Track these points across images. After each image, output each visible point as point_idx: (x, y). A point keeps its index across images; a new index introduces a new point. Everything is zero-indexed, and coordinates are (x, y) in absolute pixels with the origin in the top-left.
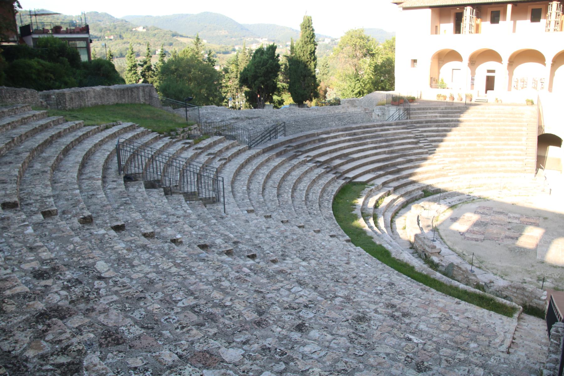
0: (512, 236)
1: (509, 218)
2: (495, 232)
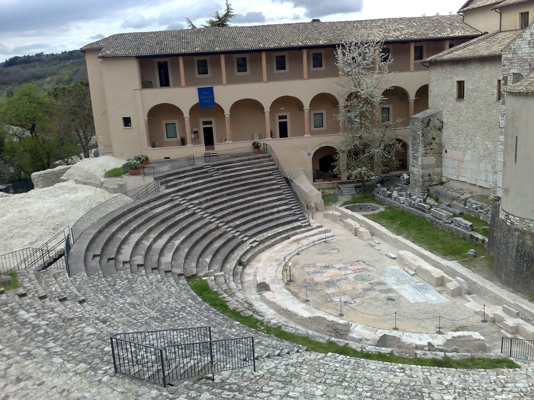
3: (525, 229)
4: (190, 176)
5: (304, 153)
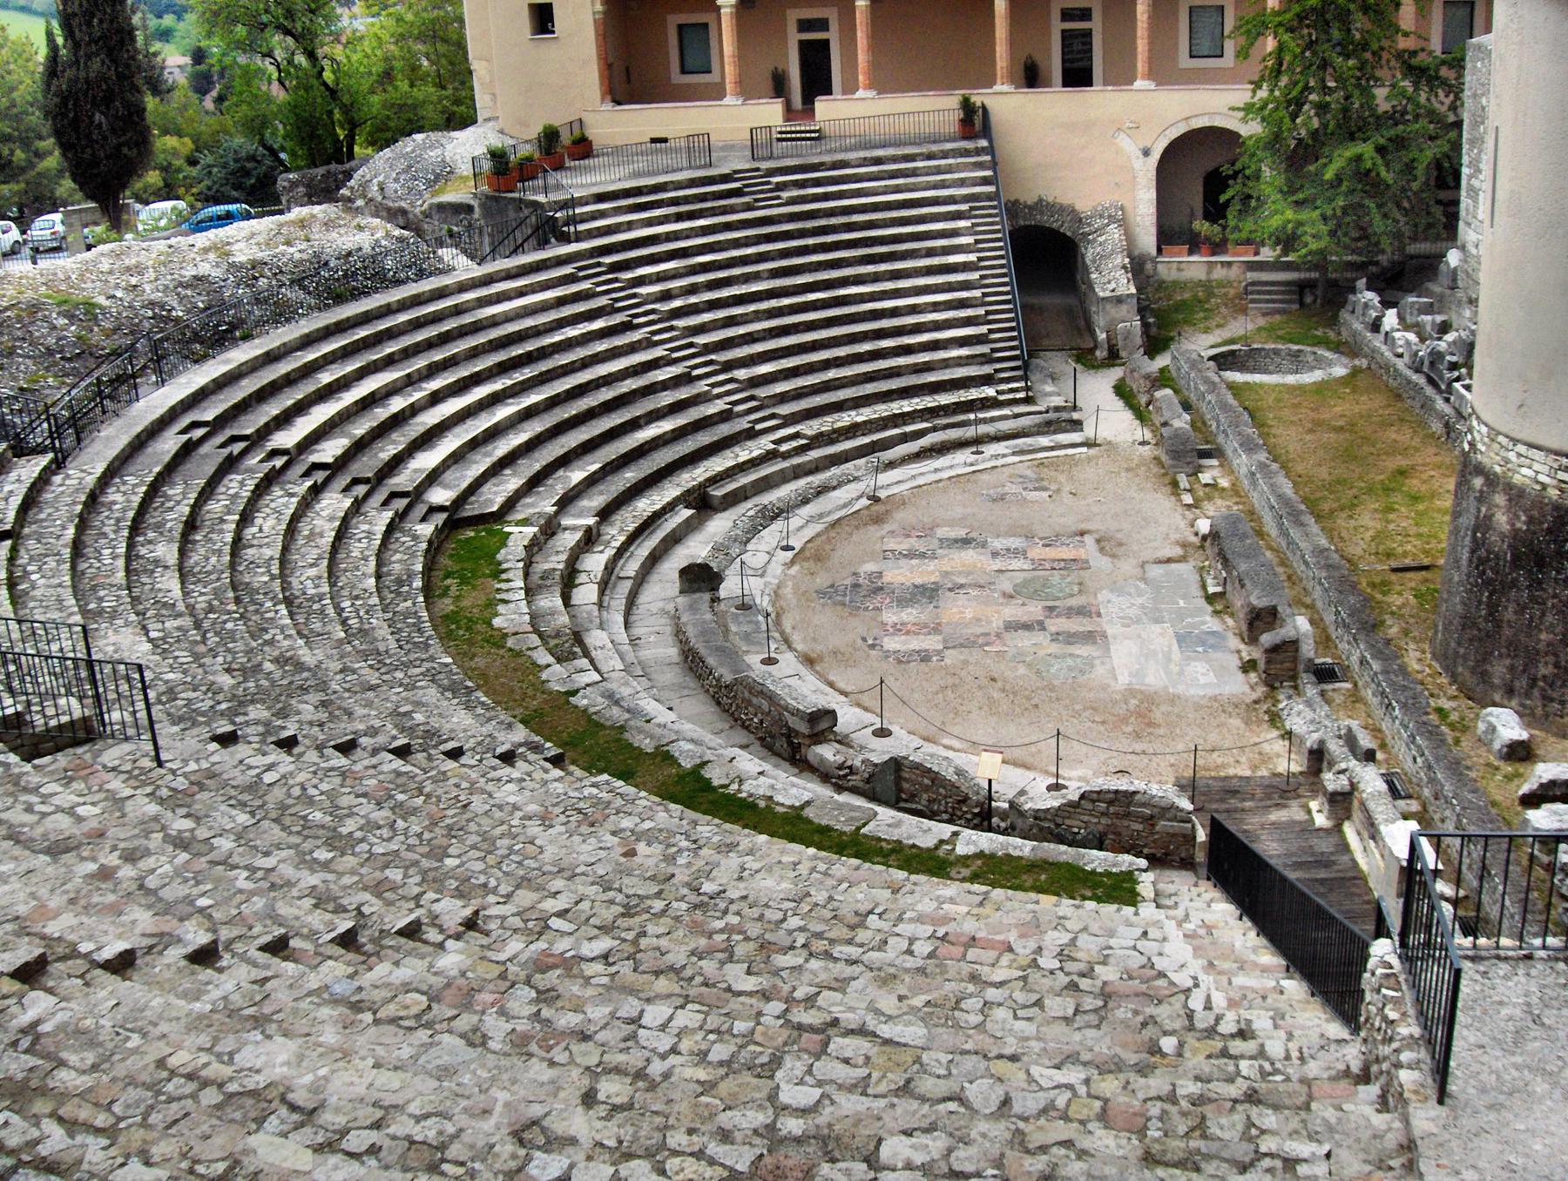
0: (1025, 619)
1: (995, 554)
2: (969, 614)
3: (1498, 469)
4: (675, 202)
5: (1129, 146)
